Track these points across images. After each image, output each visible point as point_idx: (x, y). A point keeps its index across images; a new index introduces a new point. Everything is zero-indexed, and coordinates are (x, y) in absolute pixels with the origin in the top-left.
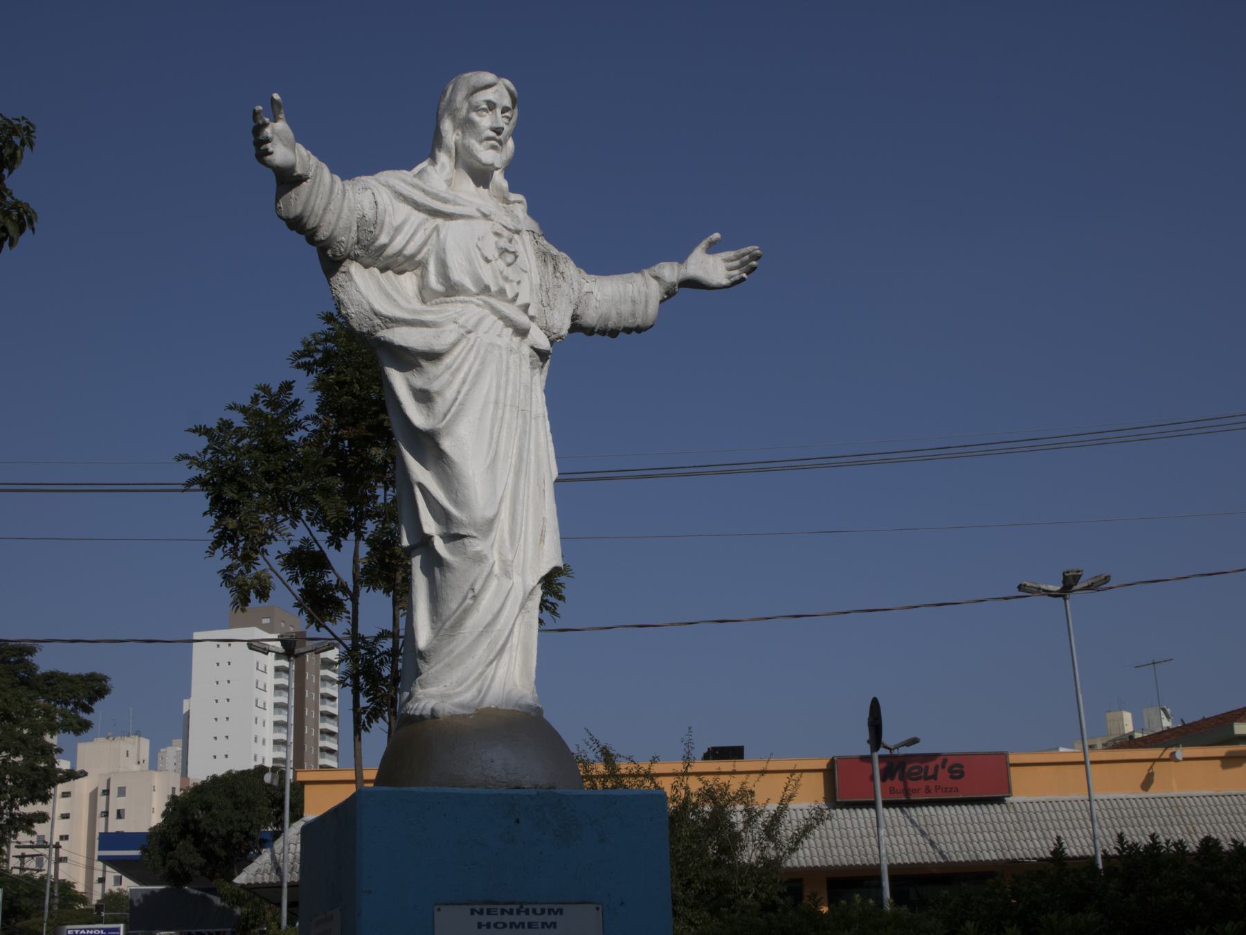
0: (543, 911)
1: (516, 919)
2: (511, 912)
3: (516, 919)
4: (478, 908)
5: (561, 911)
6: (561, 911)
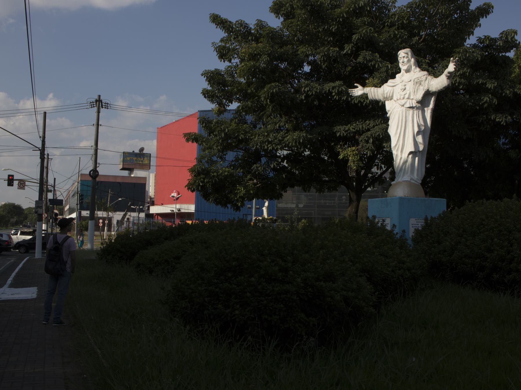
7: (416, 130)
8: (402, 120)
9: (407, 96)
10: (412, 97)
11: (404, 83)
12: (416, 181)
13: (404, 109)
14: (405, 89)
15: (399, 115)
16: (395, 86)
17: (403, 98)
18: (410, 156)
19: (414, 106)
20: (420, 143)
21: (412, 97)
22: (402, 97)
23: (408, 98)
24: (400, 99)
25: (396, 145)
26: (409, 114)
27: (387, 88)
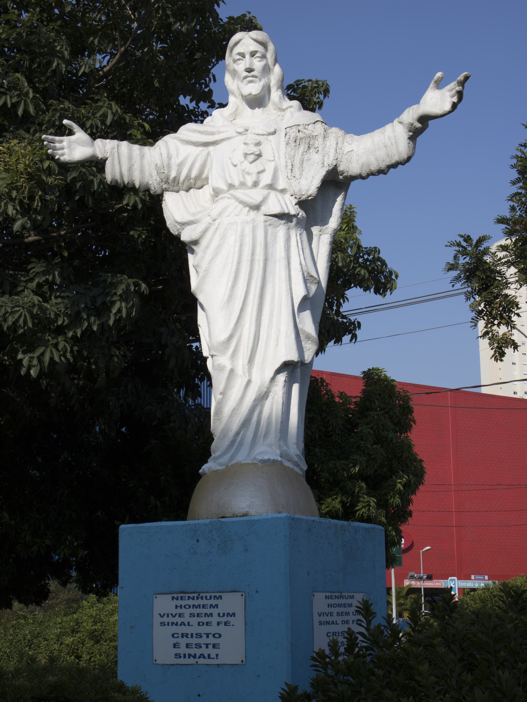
0: (211, 597)
1: (196, 602)
2: (193, 599)
3: (196, 602)
4: (175, 596)
5: (221, 597)
6: (221, 597)
7: (299, 292)
8: (253, 254)
9: (266, 179)
10: (281, 184)
11: (251, 138)
12: (298, 466)
13: (259, 218)
14: (259, 156)
15: (242, 236)
16: (214, 143)
17: (256, 184)
18: (282, 378)
19: (293, 212)
20: (308, 337)
21: (281, 184)
22: (250, 181)
23: (271, 187)
24: (243, 184)
25: (231, 337)
26: (275, 236)
27: (177, 150)
